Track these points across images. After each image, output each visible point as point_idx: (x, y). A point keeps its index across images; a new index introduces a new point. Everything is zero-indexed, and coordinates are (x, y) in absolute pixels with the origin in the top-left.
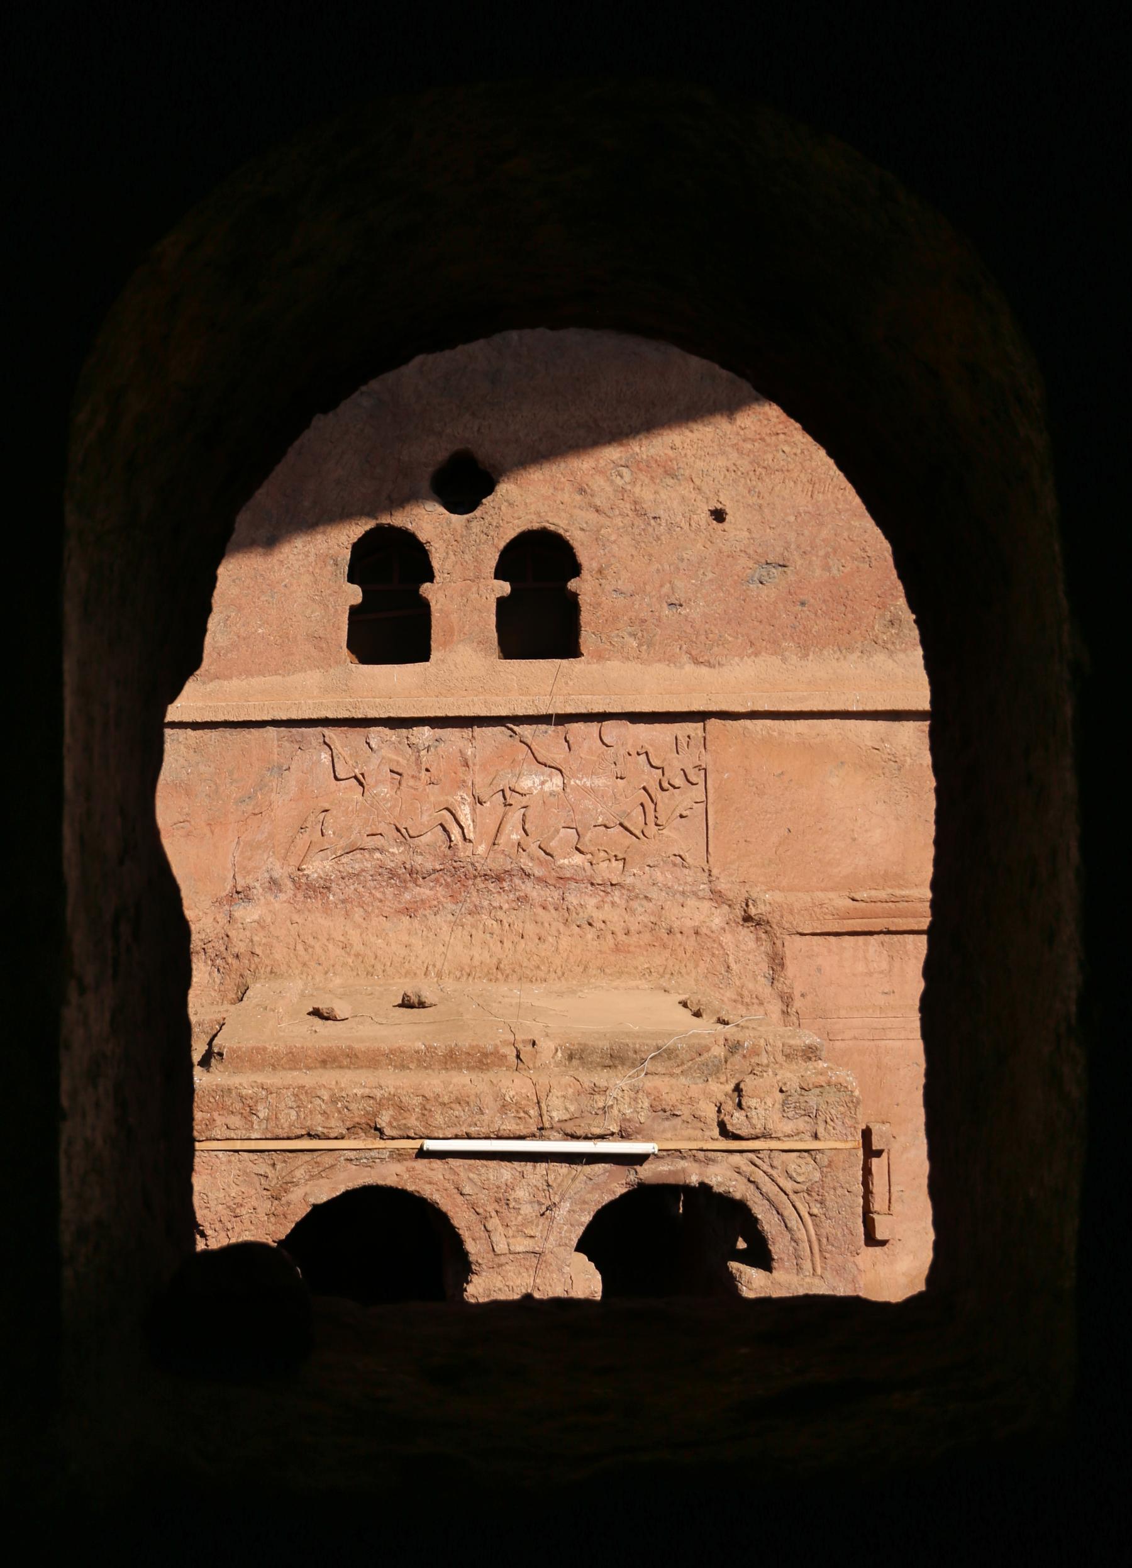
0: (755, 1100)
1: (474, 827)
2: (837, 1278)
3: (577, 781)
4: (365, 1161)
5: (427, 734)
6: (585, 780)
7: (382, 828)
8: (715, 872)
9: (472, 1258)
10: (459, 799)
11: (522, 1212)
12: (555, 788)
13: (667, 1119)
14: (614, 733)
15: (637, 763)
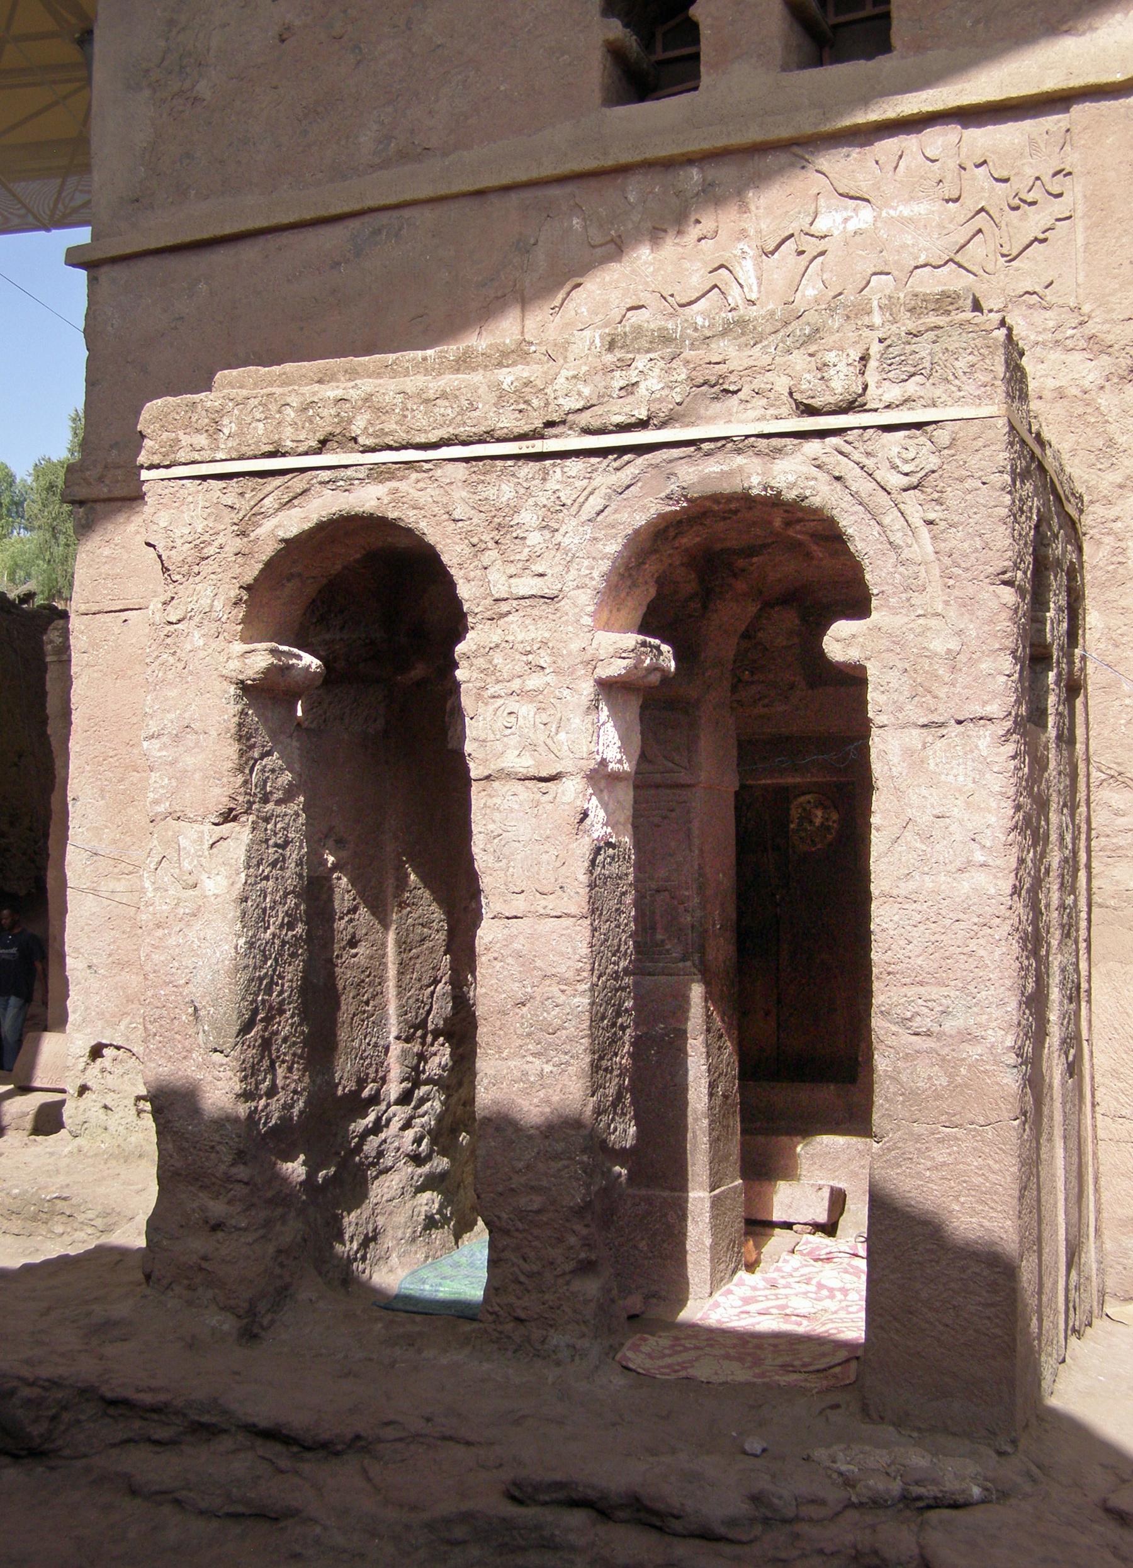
0: (833, 354)
1: (760, 285)
2: (967, 616)
3: (892, 213)
4: (341, 483)
5: (696, 178)
6: (901, 208)
7: (645, 298)
8: (1086, 309)
9: (466, 607)
10: (739, 253)
11: (528, 542)
12: (863, 226)
13: (717, 399)
14: (940, 143)
15: (974, 179)
